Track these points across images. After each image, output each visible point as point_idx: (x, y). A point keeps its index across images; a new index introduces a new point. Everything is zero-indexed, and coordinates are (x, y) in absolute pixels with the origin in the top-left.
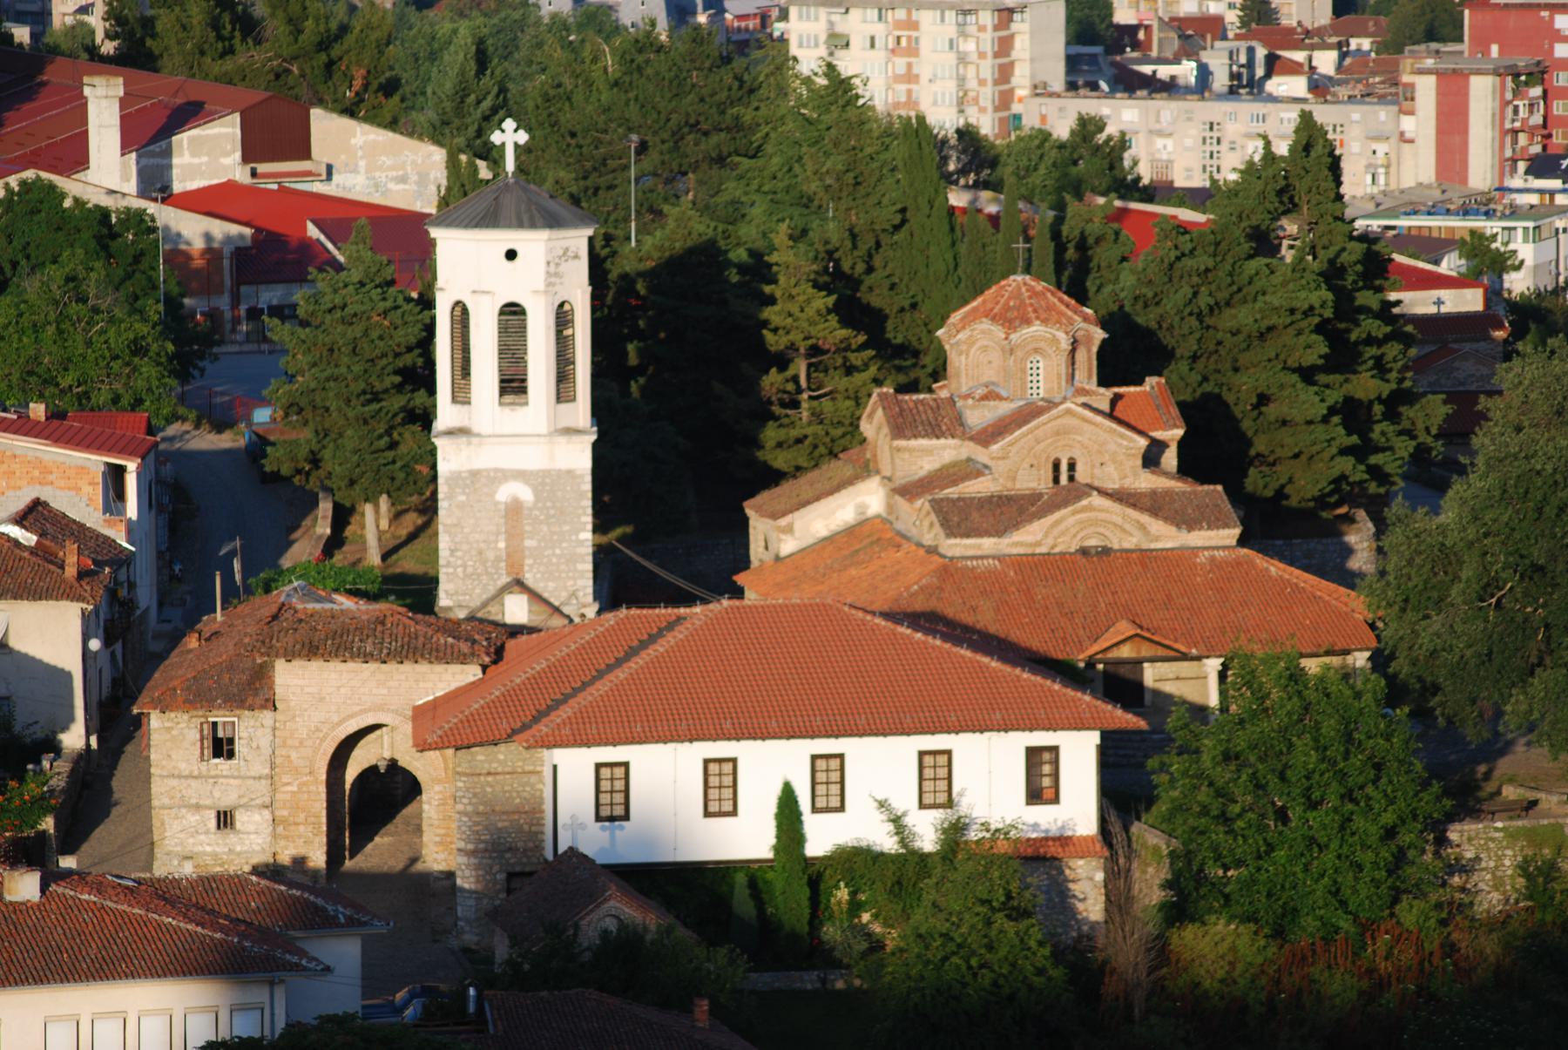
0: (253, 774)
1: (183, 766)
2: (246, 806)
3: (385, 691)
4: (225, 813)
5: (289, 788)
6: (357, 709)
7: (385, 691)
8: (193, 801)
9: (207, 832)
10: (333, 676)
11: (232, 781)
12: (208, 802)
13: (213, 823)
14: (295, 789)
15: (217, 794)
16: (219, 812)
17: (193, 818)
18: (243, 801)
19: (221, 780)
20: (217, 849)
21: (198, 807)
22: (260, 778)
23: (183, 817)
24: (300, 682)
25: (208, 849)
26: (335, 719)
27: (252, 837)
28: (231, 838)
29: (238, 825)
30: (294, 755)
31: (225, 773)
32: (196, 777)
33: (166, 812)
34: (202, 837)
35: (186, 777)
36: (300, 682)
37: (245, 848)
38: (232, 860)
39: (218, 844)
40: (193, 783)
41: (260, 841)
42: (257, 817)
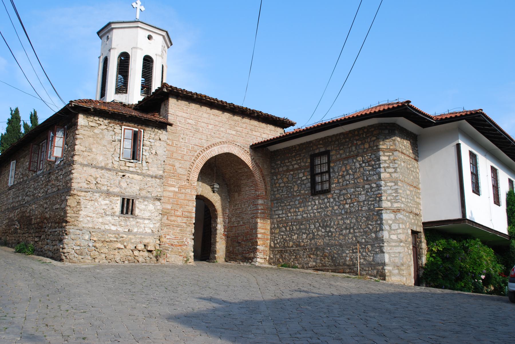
0: (151, 173)
1: (100, 158)
2: (145, 198)
3: (234, 133)
4: (128, 200)
5: (172, 189)
6: (218, 140)
7: (234, 133)
8: (105, 188)
9: (113, 214)
10: (205, 115)
11: (136, 176)
12: (116, 190)
13: (118, 208)
14: (176, 190)
15: (124, 185)
16: (123, 199)
17: (103, 202)
18: (144, 193)
19: (127, 175)
20: (120, 229)
21: (108, 194)
22: (156, 177)
23: (96, 200)
24: (185, 115)
25: (113, 228)
26: (205, 146)
27: (146, 222)
28: (132, 222)
29: (137, 212)
30: (177, 165)
31: (131, 169)
32: (109, 170)
33: (83, 194)
34: (110, 218)
35: (102, 168)
36: (185, 115)
37: (141, 230)
38: (131, 239)
39: (120, 225)
40: (107, 174)
41: (152, 226)
42: (151, 207)
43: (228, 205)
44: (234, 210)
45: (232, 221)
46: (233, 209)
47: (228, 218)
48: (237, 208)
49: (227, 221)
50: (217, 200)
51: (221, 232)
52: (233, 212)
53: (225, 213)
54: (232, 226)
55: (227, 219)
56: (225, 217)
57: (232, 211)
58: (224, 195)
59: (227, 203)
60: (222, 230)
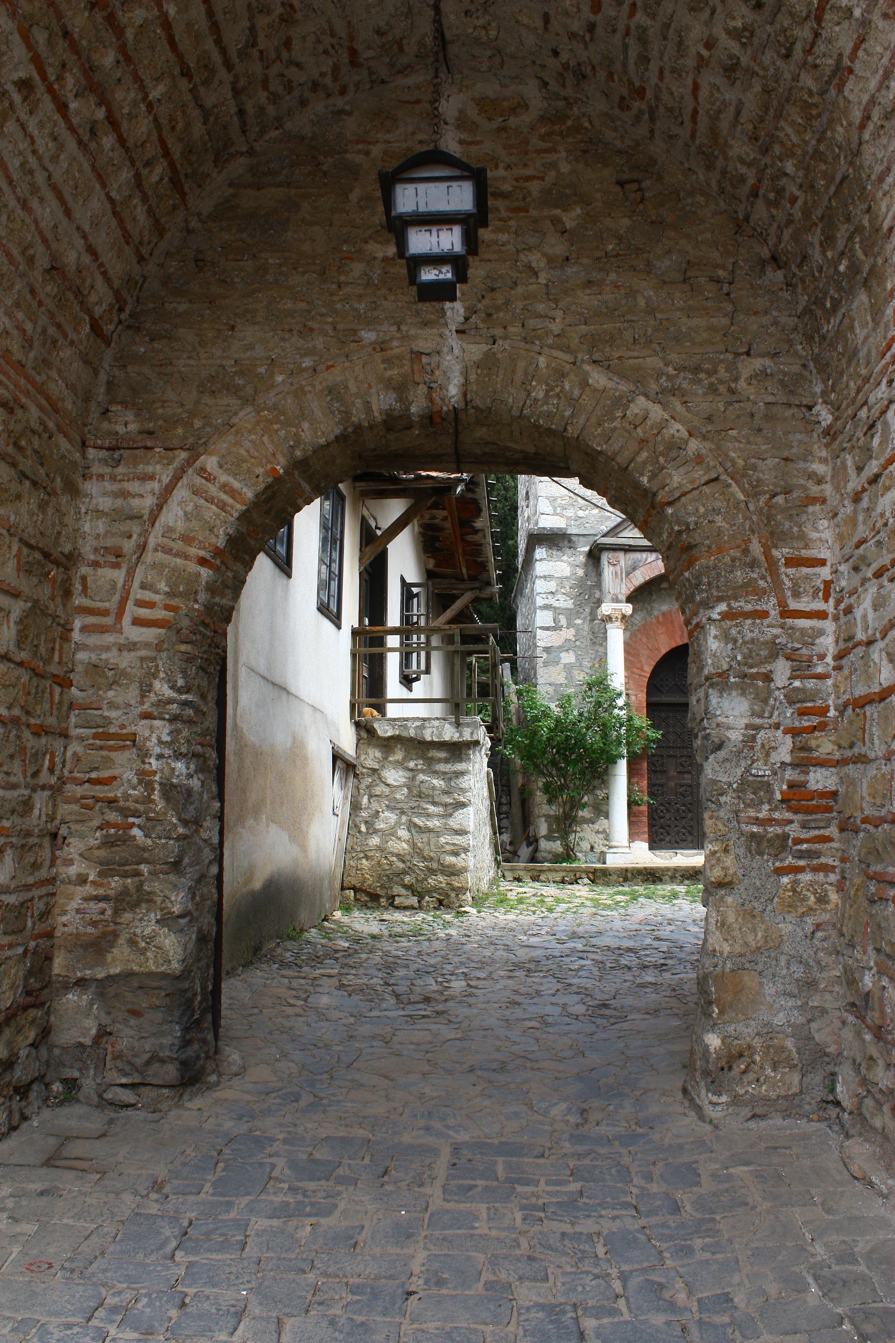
43: (819, 468)
44: (865, 503)
45: (860, 636)
46: (857, 498)
47: (829, 607)
48: (873, 467)
49: (828, 643)
50: (677, 429)
51: (761, 770)
52: (862, 531)
53: (791, 562)
54: (860, 691)
55: (829, 625)
56: (793, 605)
57: (852, 521)
58: (764, 375)
59: (807, 456)
60: (768, 751)
